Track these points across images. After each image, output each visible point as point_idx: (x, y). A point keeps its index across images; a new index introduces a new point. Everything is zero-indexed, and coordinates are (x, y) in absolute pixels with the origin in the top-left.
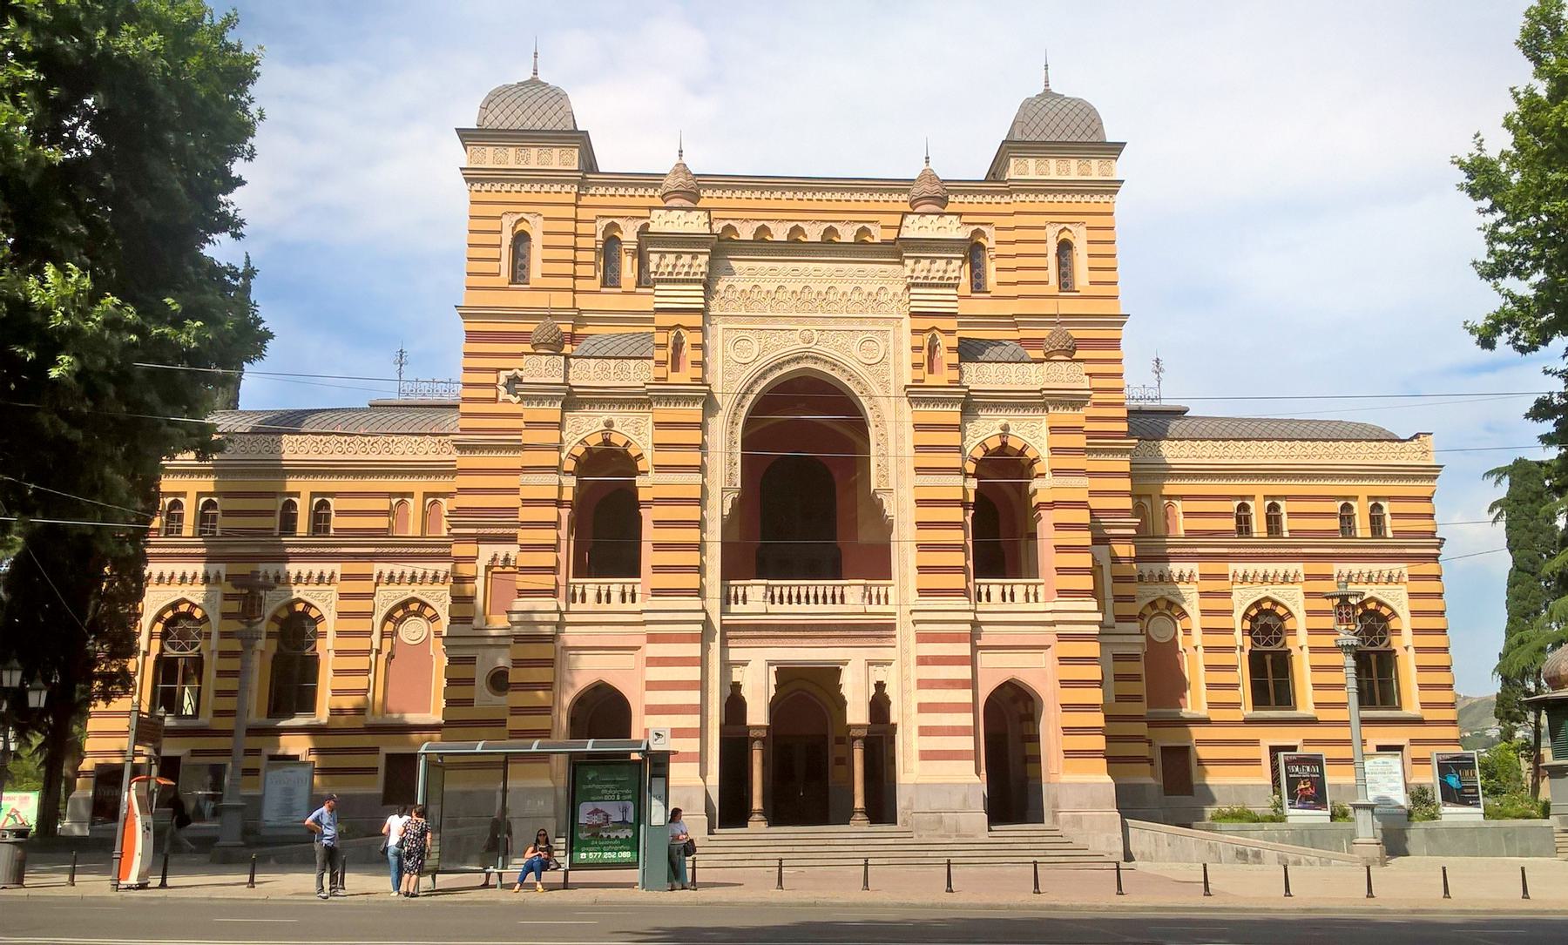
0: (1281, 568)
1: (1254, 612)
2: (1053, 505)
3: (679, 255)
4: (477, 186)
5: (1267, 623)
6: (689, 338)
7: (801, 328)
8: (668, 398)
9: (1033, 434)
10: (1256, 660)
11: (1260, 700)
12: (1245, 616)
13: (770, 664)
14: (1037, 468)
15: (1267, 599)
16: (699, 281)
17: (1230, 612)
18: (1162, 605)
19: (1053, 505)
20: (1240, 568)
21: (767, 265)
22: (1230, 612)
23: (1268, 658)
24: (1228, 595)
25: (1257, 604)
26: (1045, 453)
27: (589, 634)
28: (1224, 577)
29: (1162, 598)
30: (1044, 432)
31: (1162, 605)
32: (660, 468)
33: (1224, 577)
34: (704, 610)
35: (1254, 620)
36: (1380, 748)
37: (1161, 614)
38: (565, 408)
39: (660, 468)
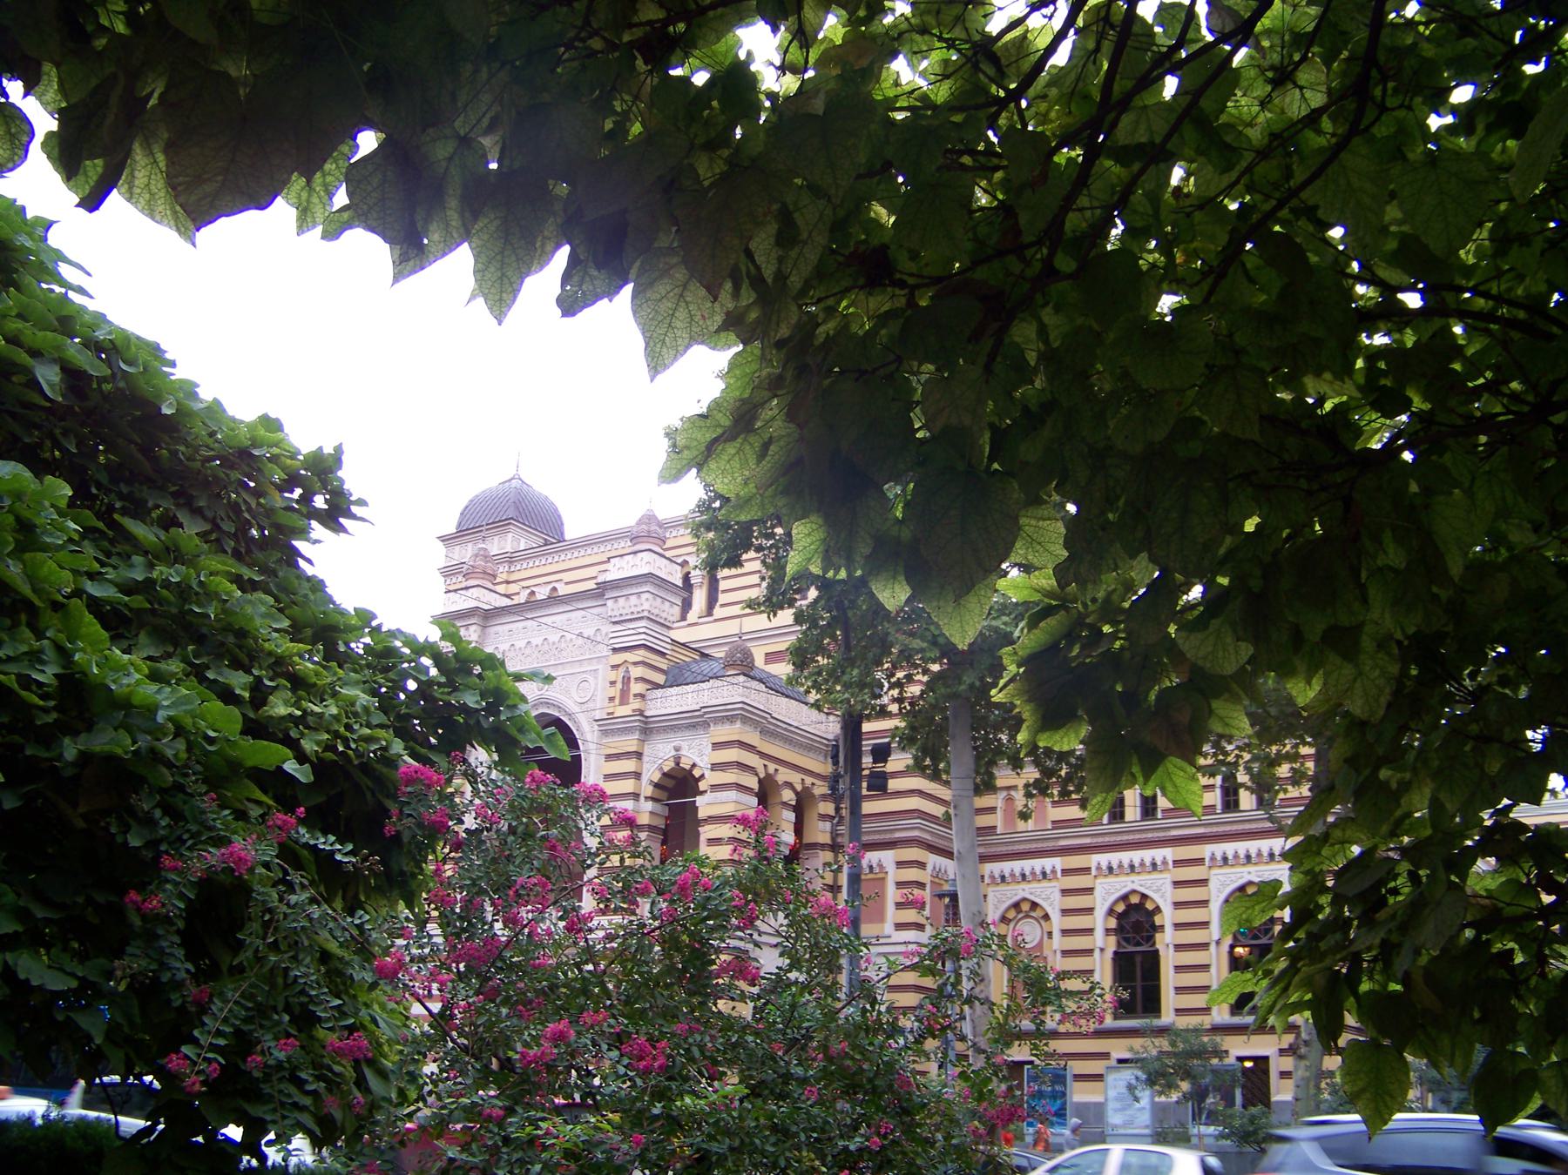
0: (1147, 855)
1: (1120, 908)
5: (1135, 921)
9: (697, 752)
10: (1123, 964)
11: (1124, 1008)
12: (1111, 912)
14: (702, 786)
15: (1134, 891)
17: (1089, 911)
18: (1025, 907)
20: (1103, 859)
22: (1089, 911)
23: (1138, 959)
24: (1089, 891)
25: (1125, 898)
28: (1086, 870)
29: (1024, 899)
31: (1025, 907)
33: (1086, 870)
35: (1120, 917)
36: (1120, 1061)
37: (1027, 916)
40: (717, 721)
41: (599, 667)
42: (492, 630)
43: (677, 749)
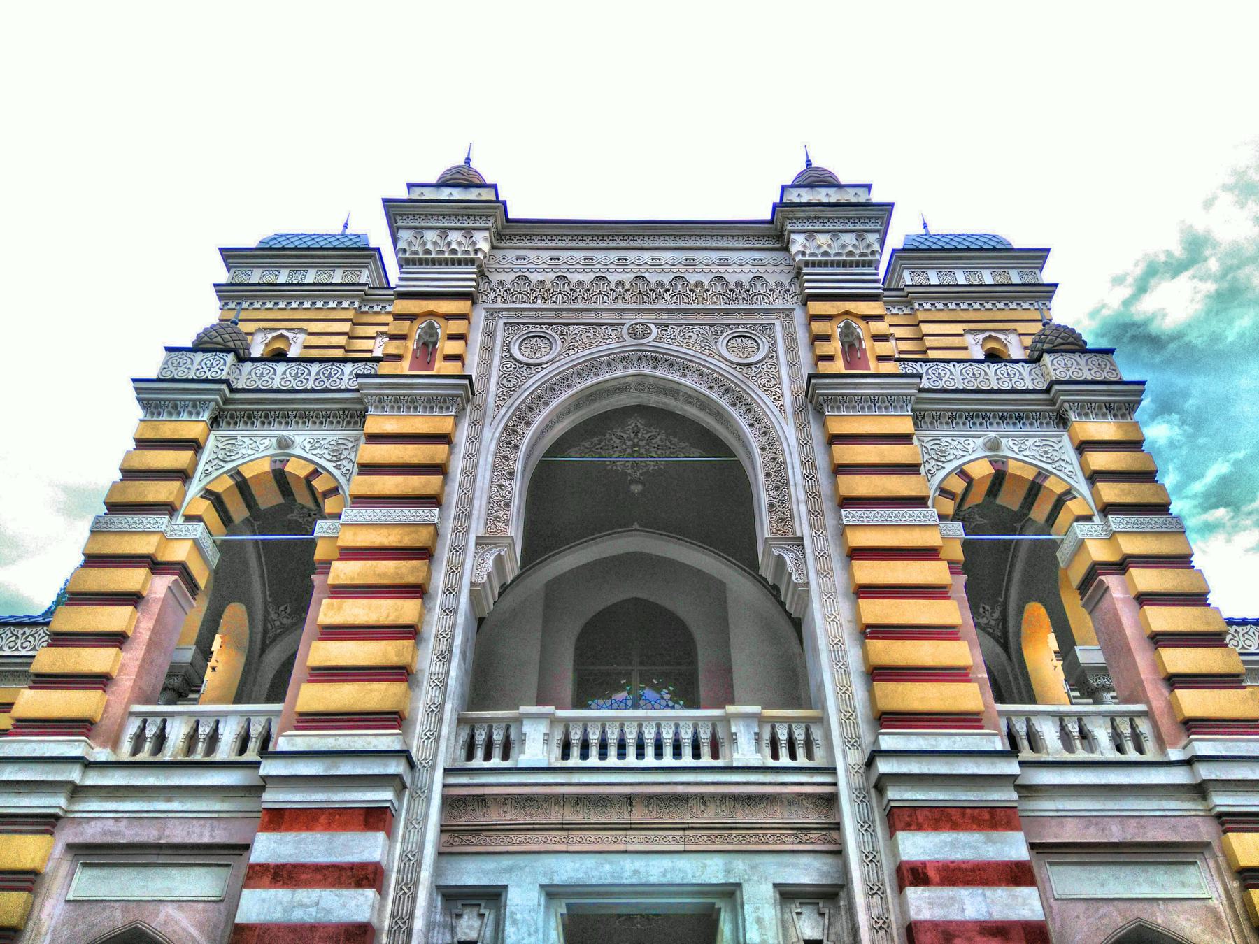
2: (1121, 566)
3: (444, 232)
4: (232, 305)
6: (443, 328)
7: (628, 322)
8: (397, 399)
13: (552, 892)
16: (472, 262)
19: (1121, 566)
21: (579, 255)
26: (1082, 487)
27: (135, 818)
30: (1071, 455)
32: (361, 501)
34: (405, 754)
38: (215, 422)
39: (361, 501)
40: (1087, 410)
41: (777, 322)
42: (512, 255)
43: (994, 446)
